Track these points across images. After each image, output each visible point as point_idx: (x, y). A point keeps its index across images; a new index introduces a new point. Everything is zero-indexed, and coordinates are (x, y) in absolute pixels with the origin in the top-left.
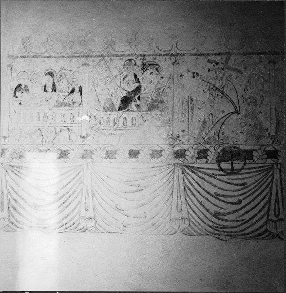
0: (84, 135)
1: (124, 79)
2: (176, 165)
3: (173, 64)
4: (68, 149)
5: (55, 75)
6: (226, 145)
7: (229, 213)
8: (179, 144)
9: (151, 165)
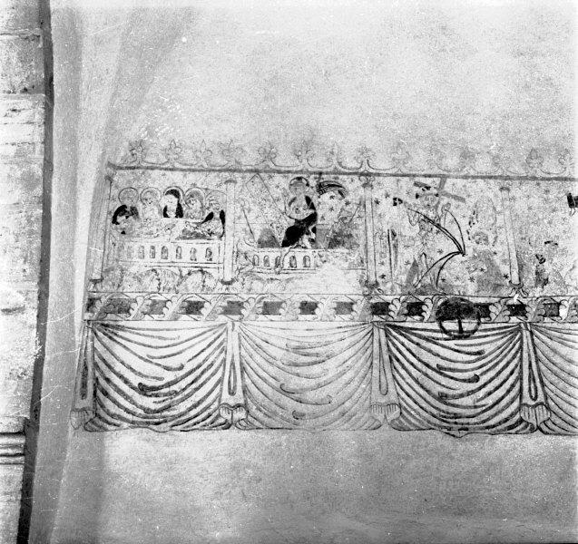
0: (228, 279)
1: (290, 204)
2: (376, 324)
3: (364, 186)
4: (201, 300)
5: (181, 194)
6: (449, 297)
7: (462, 396)
8: (377, 295)
9: (336, 324)
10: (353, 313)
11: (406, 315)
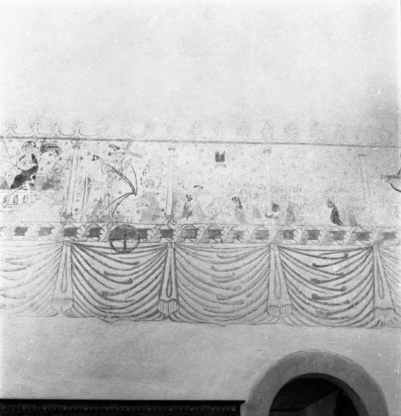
1: (20, 159)
3: (74, 147)
7: (118, 293)
8: (70, 222)
9: (37, 243)
10: (51, 235)
11: (87, 236)
